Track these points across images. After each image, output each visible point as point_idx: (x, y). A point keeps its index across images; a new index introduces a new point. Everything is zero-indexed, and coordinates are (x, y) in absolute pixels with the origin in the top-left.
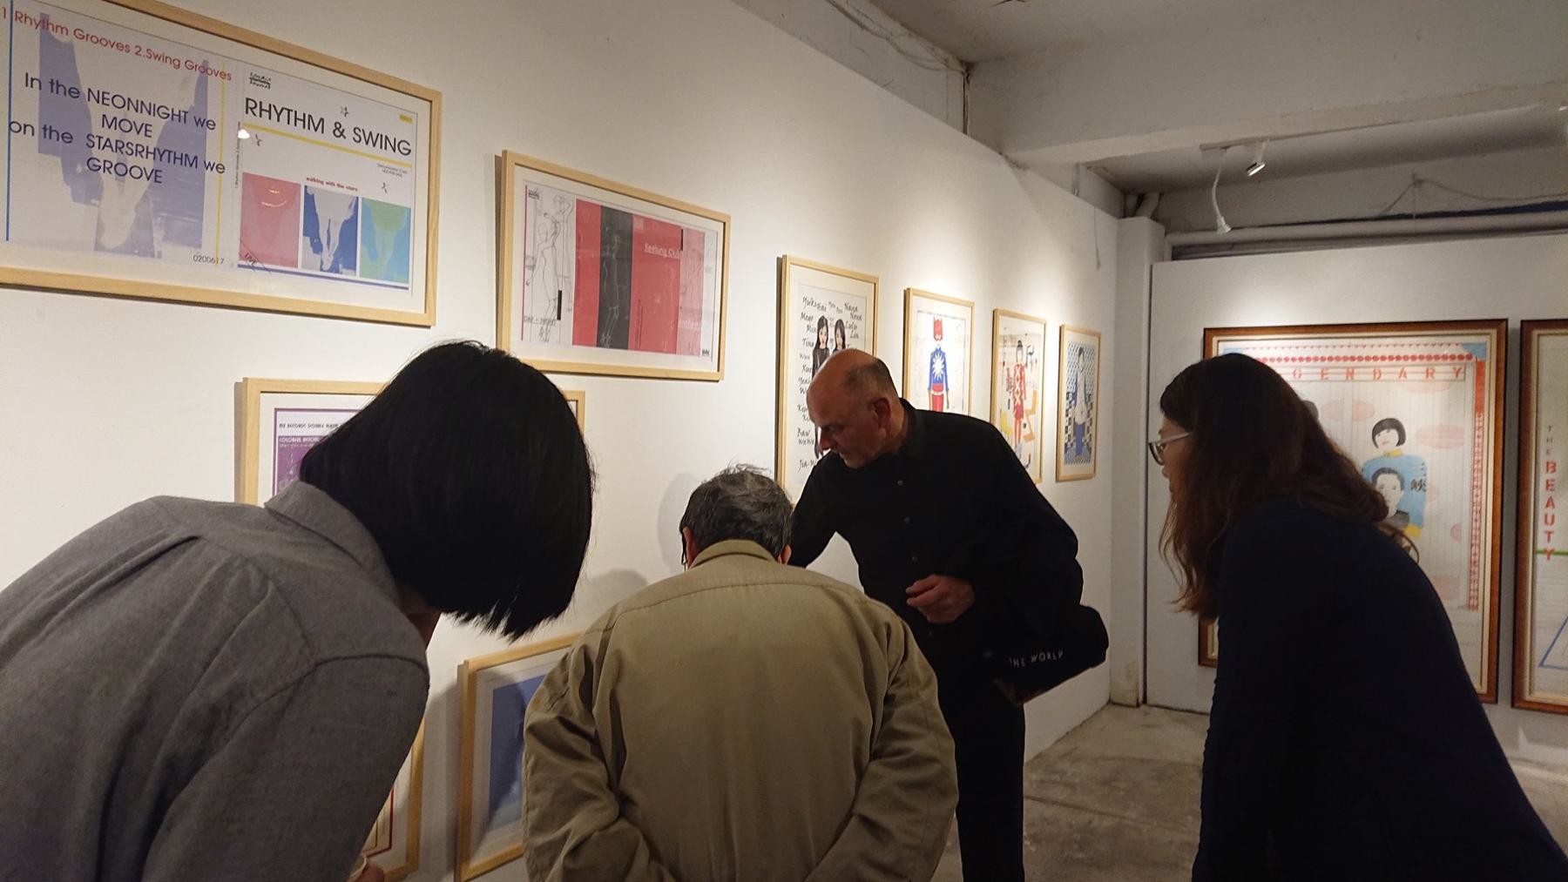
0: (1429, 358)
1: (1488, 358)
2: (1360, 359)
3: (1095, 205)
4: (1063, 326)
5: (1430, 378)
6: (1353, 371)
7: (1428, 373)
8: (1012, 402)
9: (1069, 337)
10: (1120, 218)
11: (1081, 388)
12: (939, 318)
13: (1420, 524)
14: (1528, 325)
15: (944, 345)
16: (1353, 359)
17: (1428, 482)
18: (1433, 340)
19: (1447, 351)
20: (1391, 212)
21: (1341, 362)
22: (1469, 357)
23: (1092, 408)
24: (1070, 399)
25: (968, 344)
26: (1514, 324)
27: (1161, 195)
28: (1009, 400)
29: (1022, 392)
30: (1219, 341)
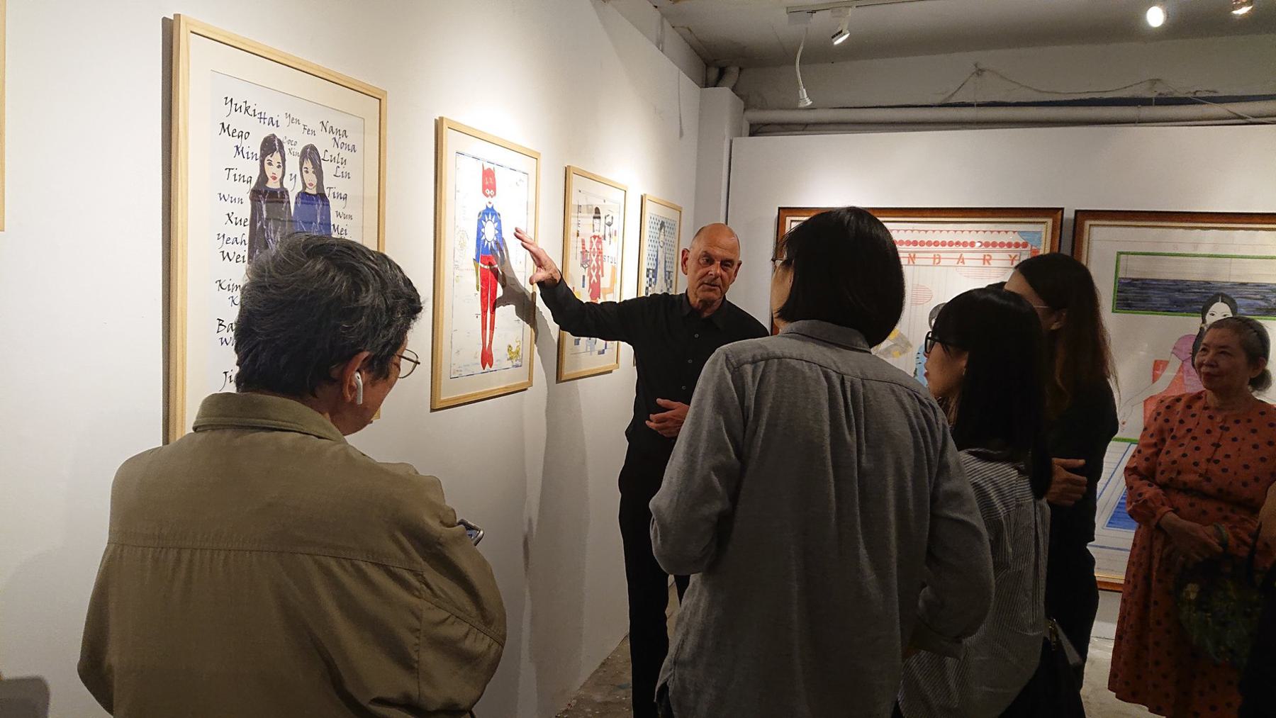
1: (1042, 247)
2: (922, 243)
3: (680, 68)
4: (645, 195)
5: (987, 265)
6: (914, 255)
7: (984, 259)
8: (587, 279)
9: (650, 209)
10: (706, 84)
11: (661, 266)
12: (491, 167)
14: (1081, 215)
15: (498, 204)
16: (915, 243)
18: (992, 227)
19: (1006, 238)
20: (953, 100)
21: (933, 246)
22: (1025, 245)
23: (671, 287)
24: (651, 276)
25: (532, 211)
26: (1069, 215)
27: (740, 69)
28: (584, 277)
29: (600, 267)
30: (792, 221)
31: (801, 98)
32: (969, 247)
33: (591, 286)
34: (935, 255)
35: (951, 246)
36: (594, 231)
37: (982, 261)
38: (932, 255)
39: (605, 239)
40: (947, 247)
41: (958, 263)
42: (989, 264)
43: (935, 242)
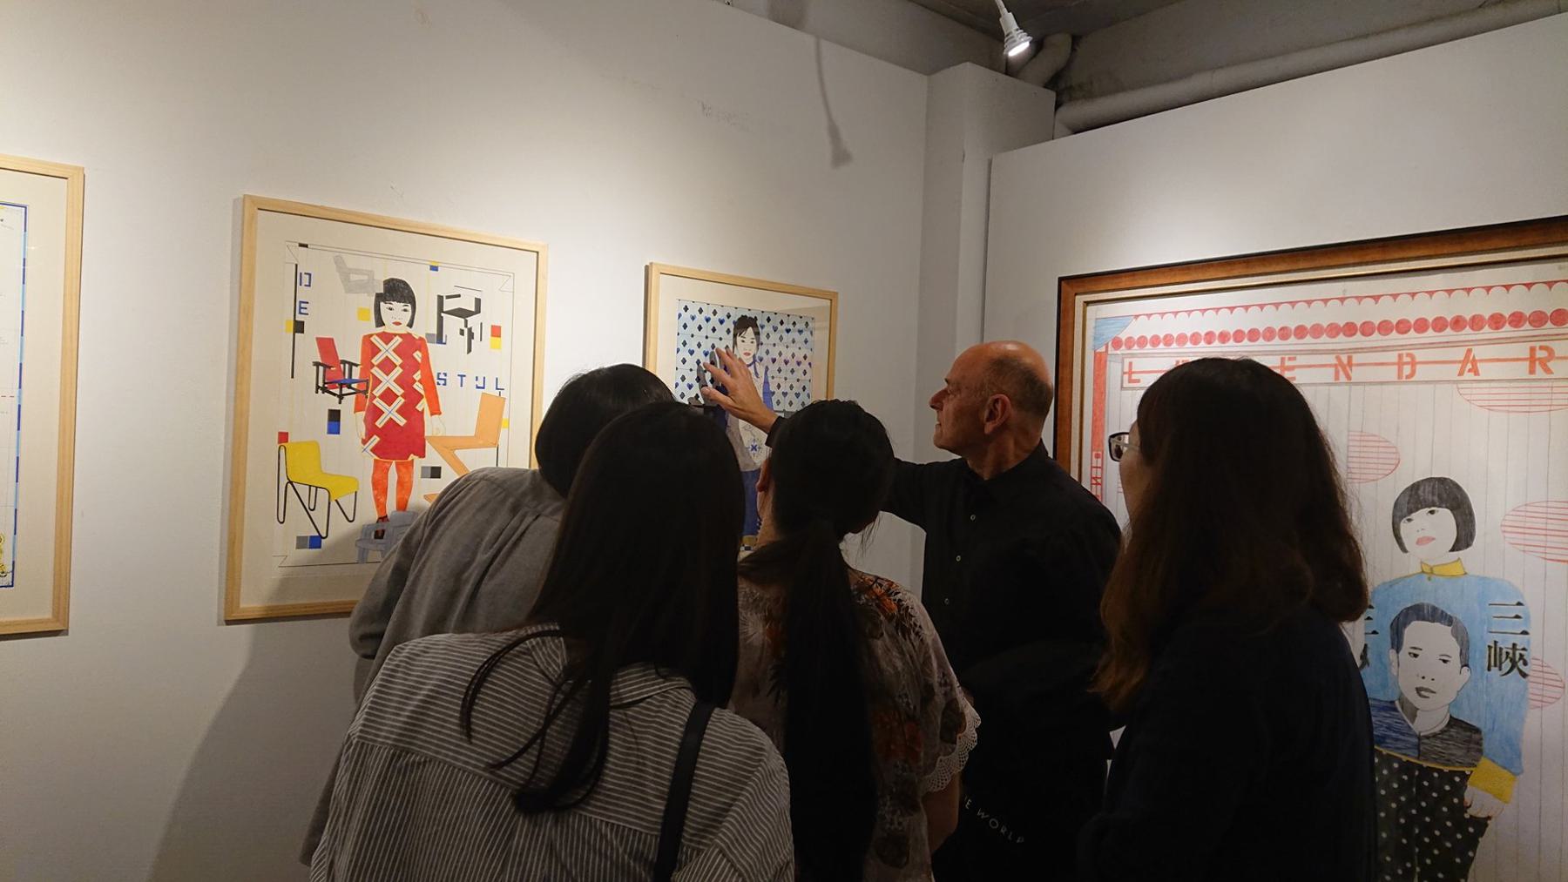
0: (1538, 319)
4: (651, 264)
6: (1350, 359)
7: (1532, 359)
13: (1512, 762)
16: (1350, 329)
17: (1533, 654)
27: (1076, 40)
28: (334, 416)
30: (1087, 303)
31: (1006, 34)
32: (1486, 329)
33: (372, 431)
34: (1400, 356)
35: (1440, 330)
36: (380, 323)
37: (1527, 363)
38: (1392, 357)
39: (440, 338)
40: (1430, 332)
41: (1461, 374)
42: (1548, 371)
43: (1400, 322)
